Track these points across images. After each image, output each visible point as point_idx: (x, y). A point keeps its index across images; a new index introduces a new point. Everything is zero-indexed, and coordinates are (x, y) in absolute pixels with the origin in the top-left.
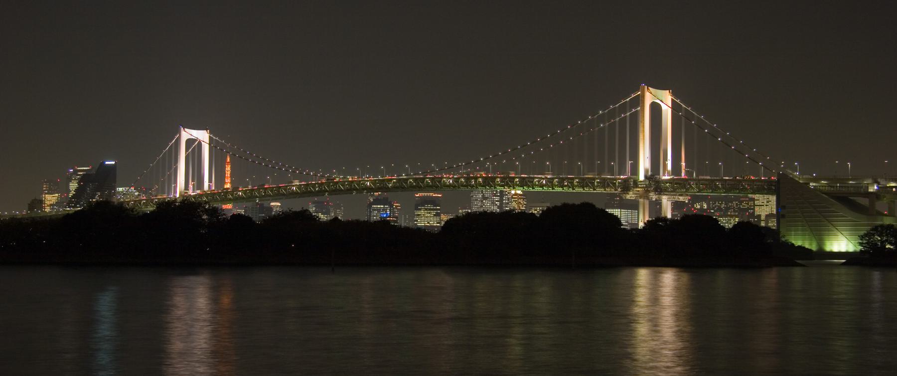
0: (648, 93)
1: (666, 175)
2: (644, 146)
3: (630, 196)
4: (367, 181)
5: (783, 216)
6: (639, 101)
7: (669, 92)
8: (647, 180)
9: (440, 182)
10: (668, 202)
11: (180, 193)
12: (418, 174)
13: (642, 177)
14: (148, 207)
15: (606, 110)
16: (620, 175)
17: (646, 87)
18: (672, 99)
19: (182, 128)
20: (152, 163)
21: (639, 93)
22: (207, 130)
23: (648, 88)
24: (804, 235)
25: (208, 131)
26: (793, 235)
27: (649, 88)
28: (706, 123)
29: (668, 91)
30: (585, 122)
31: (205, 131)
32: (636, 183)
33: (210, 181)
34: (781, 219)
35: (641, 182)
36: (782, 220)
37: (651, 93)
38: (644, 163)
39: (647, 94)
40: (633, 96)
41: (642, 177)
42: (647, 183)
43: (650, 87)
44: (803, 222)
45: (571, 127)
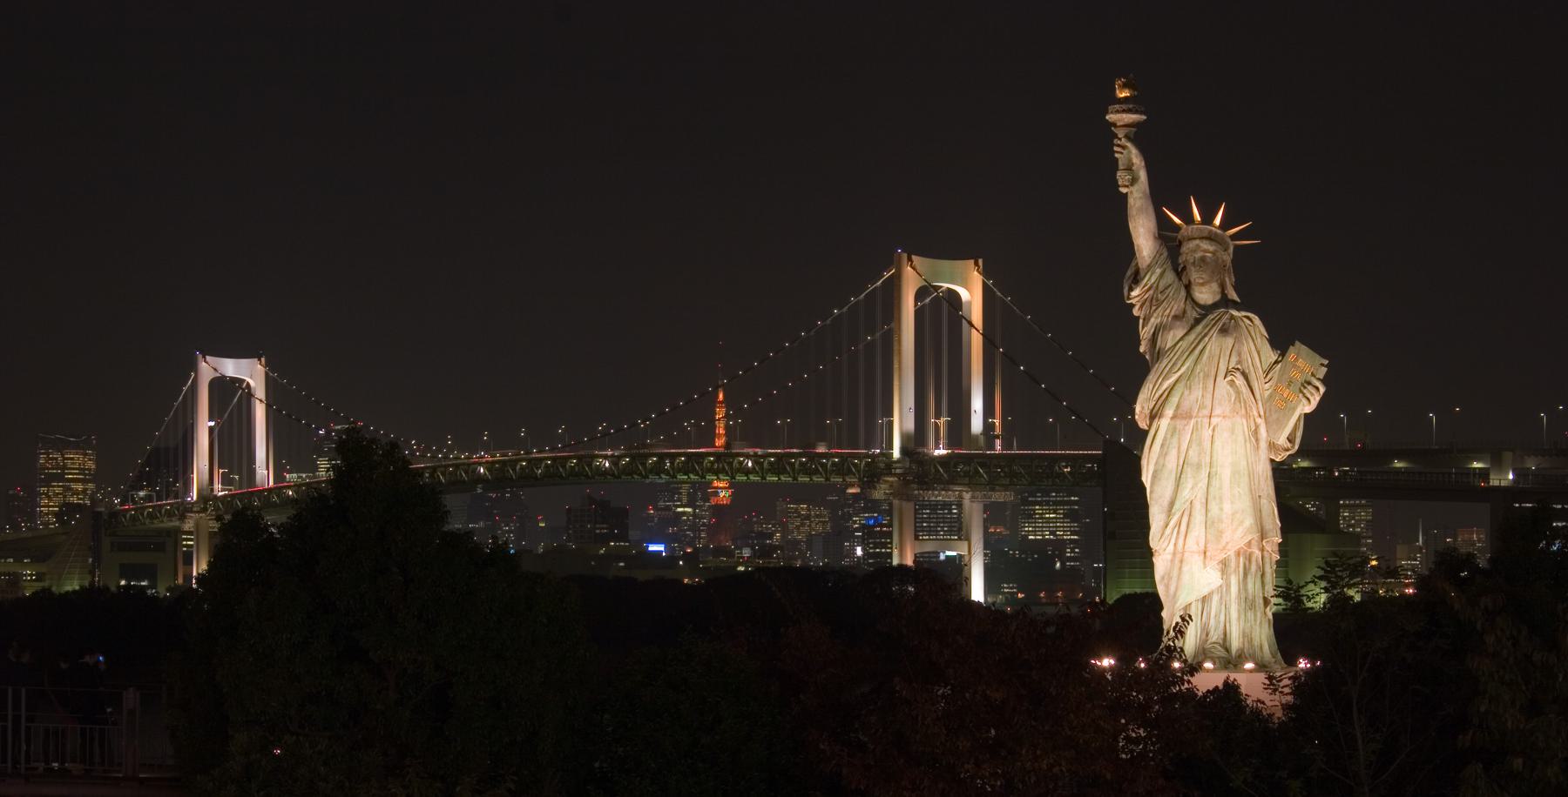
0: (909, 268)
1: (941, 446)
2: (900, 389)
3: (879, 493)
4: (480, 464)
7: (976, 264)
8: (907, 459)
9: (590, 465)
10: (975, 505)
12: (545, 451)
13: (896, 453)
14: (155, 521)
16: (868, 447)
17: (905, 255)
18: (983, 282)
23: (910, 259)
25: (263, 359)
27: (914, 257)
29: (972, 261)
30: (812, 333)
31: (256, 359)
32: (890, 464)
33: (268, 469)
35: (898, 461)
37: (914, 268)
38: (902, 421)
40: (886, 275)
42: (908, 465)
43: (916, 255)
45: (790, 344)
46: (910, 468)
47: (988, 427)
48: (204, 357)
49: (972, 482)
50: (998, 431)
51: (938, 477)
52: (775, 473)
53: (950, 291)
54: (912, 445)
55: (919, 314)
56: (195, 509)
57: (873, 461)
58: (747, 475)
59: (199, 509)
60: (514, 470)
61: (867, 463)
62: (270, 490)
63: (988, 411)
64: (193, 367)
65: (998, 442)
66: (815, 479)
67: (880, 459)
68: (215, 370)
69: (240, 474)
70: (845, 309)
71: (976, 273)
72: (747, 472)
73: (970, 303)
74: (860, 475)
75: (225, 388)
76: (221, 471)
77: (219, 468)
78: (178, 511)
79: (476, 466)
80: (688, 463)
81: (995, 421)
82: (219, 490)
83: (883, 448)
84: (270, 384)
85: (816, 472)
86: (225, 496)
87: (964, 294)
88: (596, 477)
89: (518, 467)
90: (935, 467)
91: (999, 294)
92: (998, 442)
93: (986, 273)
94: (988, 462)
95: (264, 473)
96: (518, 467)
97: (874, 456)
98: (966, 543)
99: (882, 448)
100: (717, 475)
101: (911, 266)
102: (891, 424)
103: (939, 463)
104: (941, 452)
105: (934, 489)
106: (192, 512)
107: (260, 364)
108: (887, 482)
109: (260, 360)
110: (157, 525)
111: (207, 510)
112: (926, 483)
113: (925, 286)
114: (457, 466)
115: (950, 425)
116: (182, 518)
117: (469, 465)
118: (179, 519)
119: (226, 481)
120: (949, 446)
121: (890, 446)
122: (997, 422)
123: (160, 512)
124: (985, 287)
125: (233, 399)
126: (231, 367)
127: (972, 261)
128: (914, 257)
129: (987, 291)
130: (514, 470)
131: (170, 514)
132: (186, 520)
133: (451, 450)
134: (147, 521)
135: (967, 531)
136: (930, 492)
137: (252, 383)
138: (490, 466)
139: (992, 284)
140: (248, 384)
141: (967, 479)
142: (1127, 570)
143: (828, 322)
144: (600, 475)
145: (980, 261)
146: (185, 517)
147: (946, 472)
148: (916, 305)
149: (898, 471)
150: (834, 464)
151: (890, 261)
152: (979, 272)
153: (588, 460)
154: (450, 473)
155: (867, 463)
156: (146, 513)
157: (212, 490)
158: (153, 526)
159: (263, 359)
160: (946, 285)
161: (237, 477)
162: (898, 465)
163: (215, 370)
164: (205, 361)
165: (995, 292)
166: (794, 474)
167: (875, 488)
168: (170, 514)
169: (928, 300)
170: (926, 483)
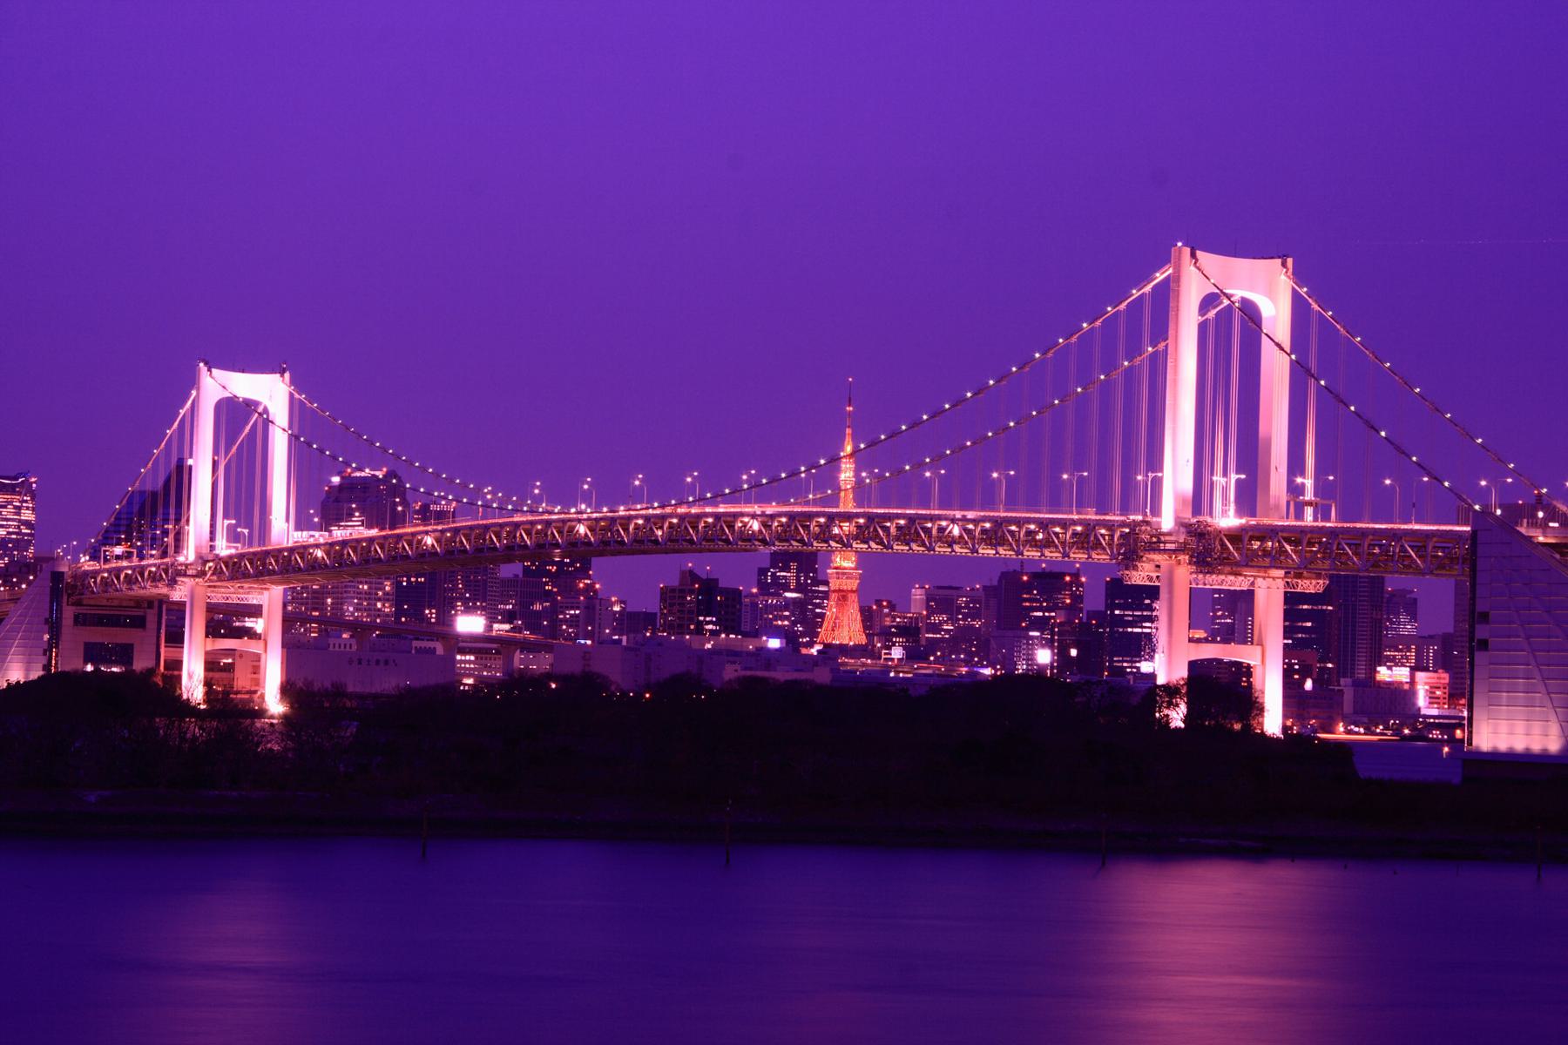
0: (1193, 268)
4: (579, 521)
5: (1484, 645)
6: (1165, 297)
7: (1284, 265)
8: (1182, 529)
9: (731, 527)
11: (197, 549)
14: (134, 587)
15: (1096, 319)
16: (1125, 510)
17: (1187, 251)
18: (1293, 289)
19: (206, 368)
20: (145, 466)
21: (1170, 271)
22: (282, 373)
23: (1193, 255)
24: (1530, 704)
25: (287, 375)
26: (1504, 702)
27: (1199, 254)
28: (1368, 356)
29: (1279, 261)
30: (1050, 355)
31: (278, 375)
33: (287, 520)
34: (1476, 653)
35: (1169, 534)
36: (1480, 657)
37: (1199, 270)
39: (1189, 271)
40: (1160, 277)
41: (1167, 522)
44: (1528, 665)
46: (1185, 543)
47: (1295, 490)
48: (209, 370)
49: (1275, 559)
50: (1309, 495)
51: (1225, 555)
52: (991, 544)
53: (1244, 301)
54: (1188, 516)
55: (1203, 327)
56: (190, 572)
57: (1132, 530)
58: (950, 546)
59: (194, 572)
60: (626, 530)
61: (1123, 536)
62: (291, 550)
63: (1296, 464)
64: (193, 381)
65: (1309, 511)
66: (1047, 553)
67: (1143, 528)
68: (224, 387)
69: (249, 525)
70: (1098, 323)
71: (1283, 277)
72: (951, 542)
73: (1274, 319)
74: (1112, 550)
75: (235, 413)
76: (227, 522)
77: (224, 518)
78: (166, 573)
79: (574, 523)
80: (868, 527)
81: (1306, 481)
82: (224, 548)
83: (1145, 515)
84: (297, 410)
85: (1048, 543)
86: (231, 557)
87: (1267, 308)
88: (740, 543)
89: (631, 527)
90: (1223, 545)
91: (1315, 306)
92: (1309, 511)
93: (1299, 276)
94: (1297, 536)
95: (282, 529)
96: (631, 527)
97: (1135, 524)
98: (1259, 649)
99: (1145, 515)
100: (908, 544)
101: (1195, 263)
102: (1157, 484)
103: (1225, 535)
104: (1227, 519)
105: (1220, 573)
106: (185, 575)
107: (283, 381)
108: (1153, 560)
109: (282, 376)
110: (137, 591)
111: (206, 575)
112: (1208, 564)
113: (1213, 294)
114: (548, 523)
115: (1238, 481)
116: (172, 583)
117: (564, 521)
118: (168, 585)
119: (233, 537)
120: (1240, 512)
121: (1156, 511)
122: (1309, 483)
123: (142, 576)
124: (1296, 298)
125: (244, 427)
126: (245, 385)
128: (1199, 254)
129: (1298, 304)
130: (626, 530)
131: (155, 578)
132: (178, 587)
133: (537, 500)
134: (124, 587)
135: (1260, 625)
136: (1214, 576)
138: (593, 525)
139: (1306, 293)
140: (266, 410)
141: (1268, 560)
142: (1505, 694)
143: (1074, 339)
144: (744, 541)
145: (1290, 261)
146: (175, 582)
147: (1237, 549)
149: (1169, 546)
150: (1075, 534)
151: (1163, 260)
152: (1289, 277)
153: (729, 519)
154: (538, 532)
155: (1123, 536)
156: (122, 576)
157: (212, 548)
158: (132, 593)
159: (287, 375)
160: (1238, 294)
161: (246, 531)
162: (1167, 538)
163: (224, 387)
164: (211, 375)
165: (1311, 305)
166: (1018, 546)
167: (1135, 568)
168: (155, 578)
169: (1212, 314)
170: (1208, 564)
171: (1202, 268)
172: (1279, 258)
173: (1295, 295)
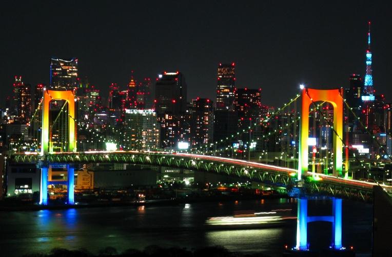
0: (306, 94)
4: (147, 155)
7: (340, 91)
29: (338, 90)
50: (347, 169)
60: (160, 160)
65: (347, 174)
70: (283, 109)
71: (339, 95)
76: (53, 143)
92: (347, 174)
98: (333, 217)
126: (58, 95)
127: (338, 90)
137: (69, 102)
148: (310, 110)
171: (310, 94)
172: (336, 89)
173: (344, 102)
